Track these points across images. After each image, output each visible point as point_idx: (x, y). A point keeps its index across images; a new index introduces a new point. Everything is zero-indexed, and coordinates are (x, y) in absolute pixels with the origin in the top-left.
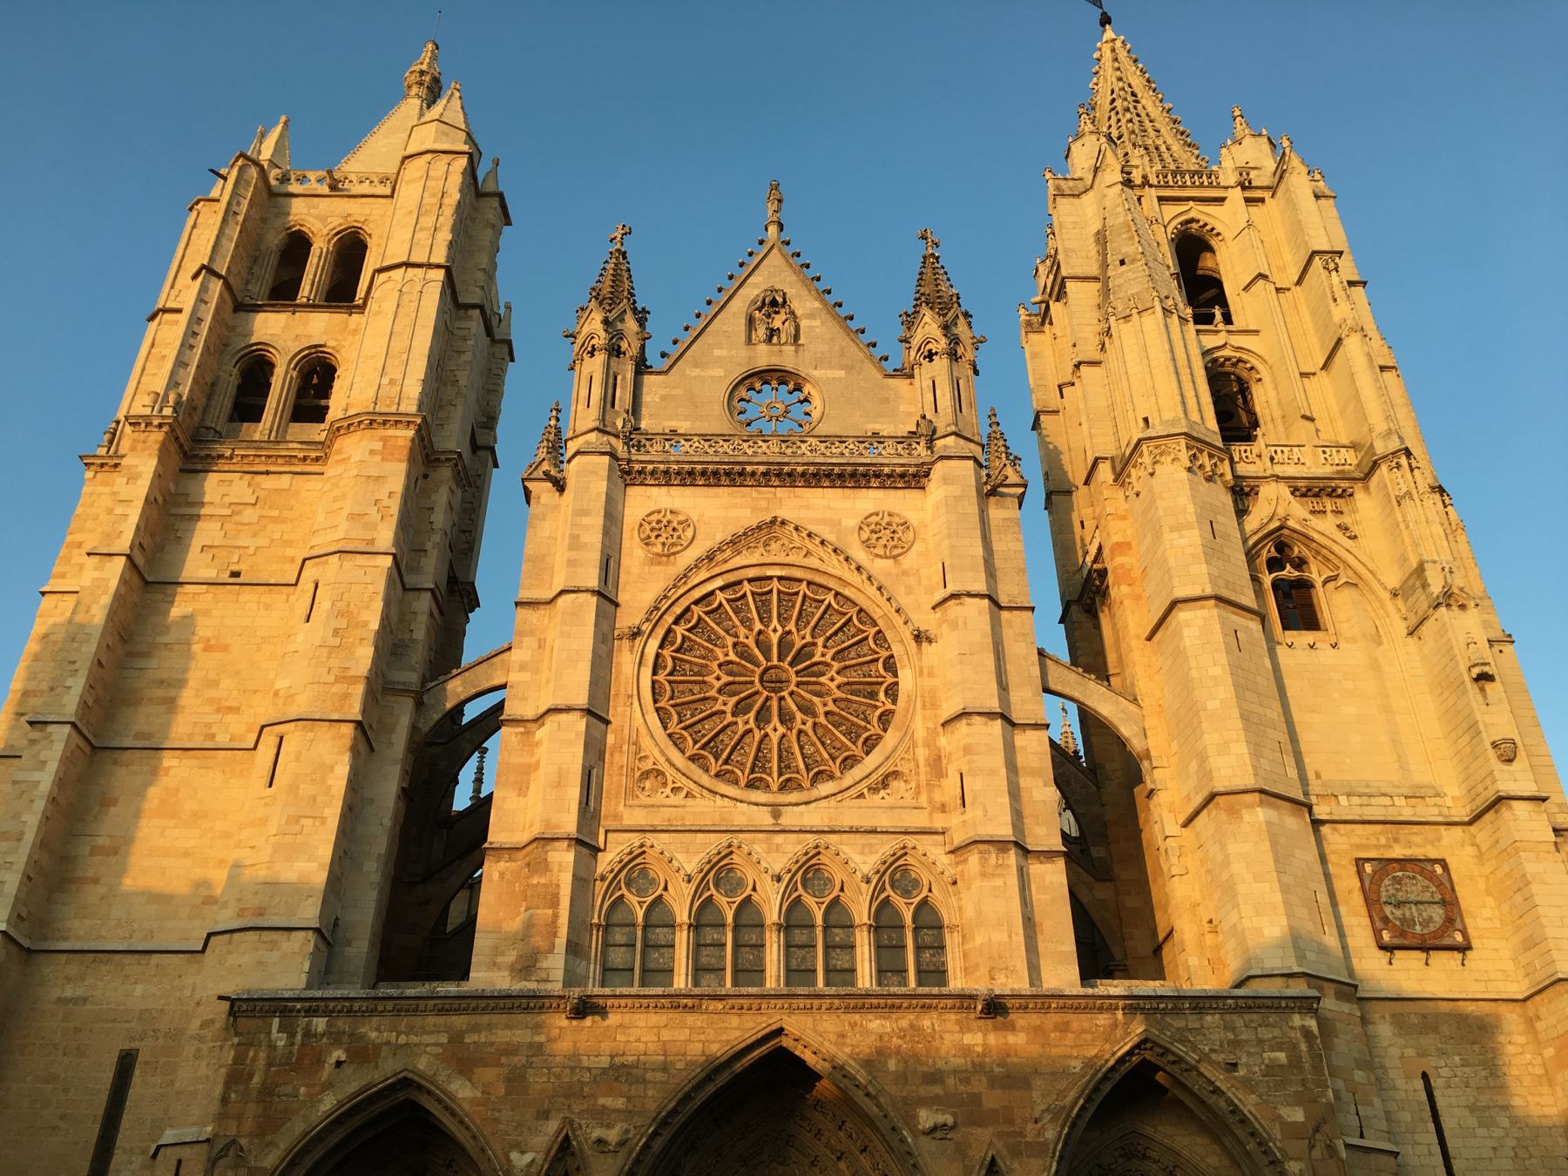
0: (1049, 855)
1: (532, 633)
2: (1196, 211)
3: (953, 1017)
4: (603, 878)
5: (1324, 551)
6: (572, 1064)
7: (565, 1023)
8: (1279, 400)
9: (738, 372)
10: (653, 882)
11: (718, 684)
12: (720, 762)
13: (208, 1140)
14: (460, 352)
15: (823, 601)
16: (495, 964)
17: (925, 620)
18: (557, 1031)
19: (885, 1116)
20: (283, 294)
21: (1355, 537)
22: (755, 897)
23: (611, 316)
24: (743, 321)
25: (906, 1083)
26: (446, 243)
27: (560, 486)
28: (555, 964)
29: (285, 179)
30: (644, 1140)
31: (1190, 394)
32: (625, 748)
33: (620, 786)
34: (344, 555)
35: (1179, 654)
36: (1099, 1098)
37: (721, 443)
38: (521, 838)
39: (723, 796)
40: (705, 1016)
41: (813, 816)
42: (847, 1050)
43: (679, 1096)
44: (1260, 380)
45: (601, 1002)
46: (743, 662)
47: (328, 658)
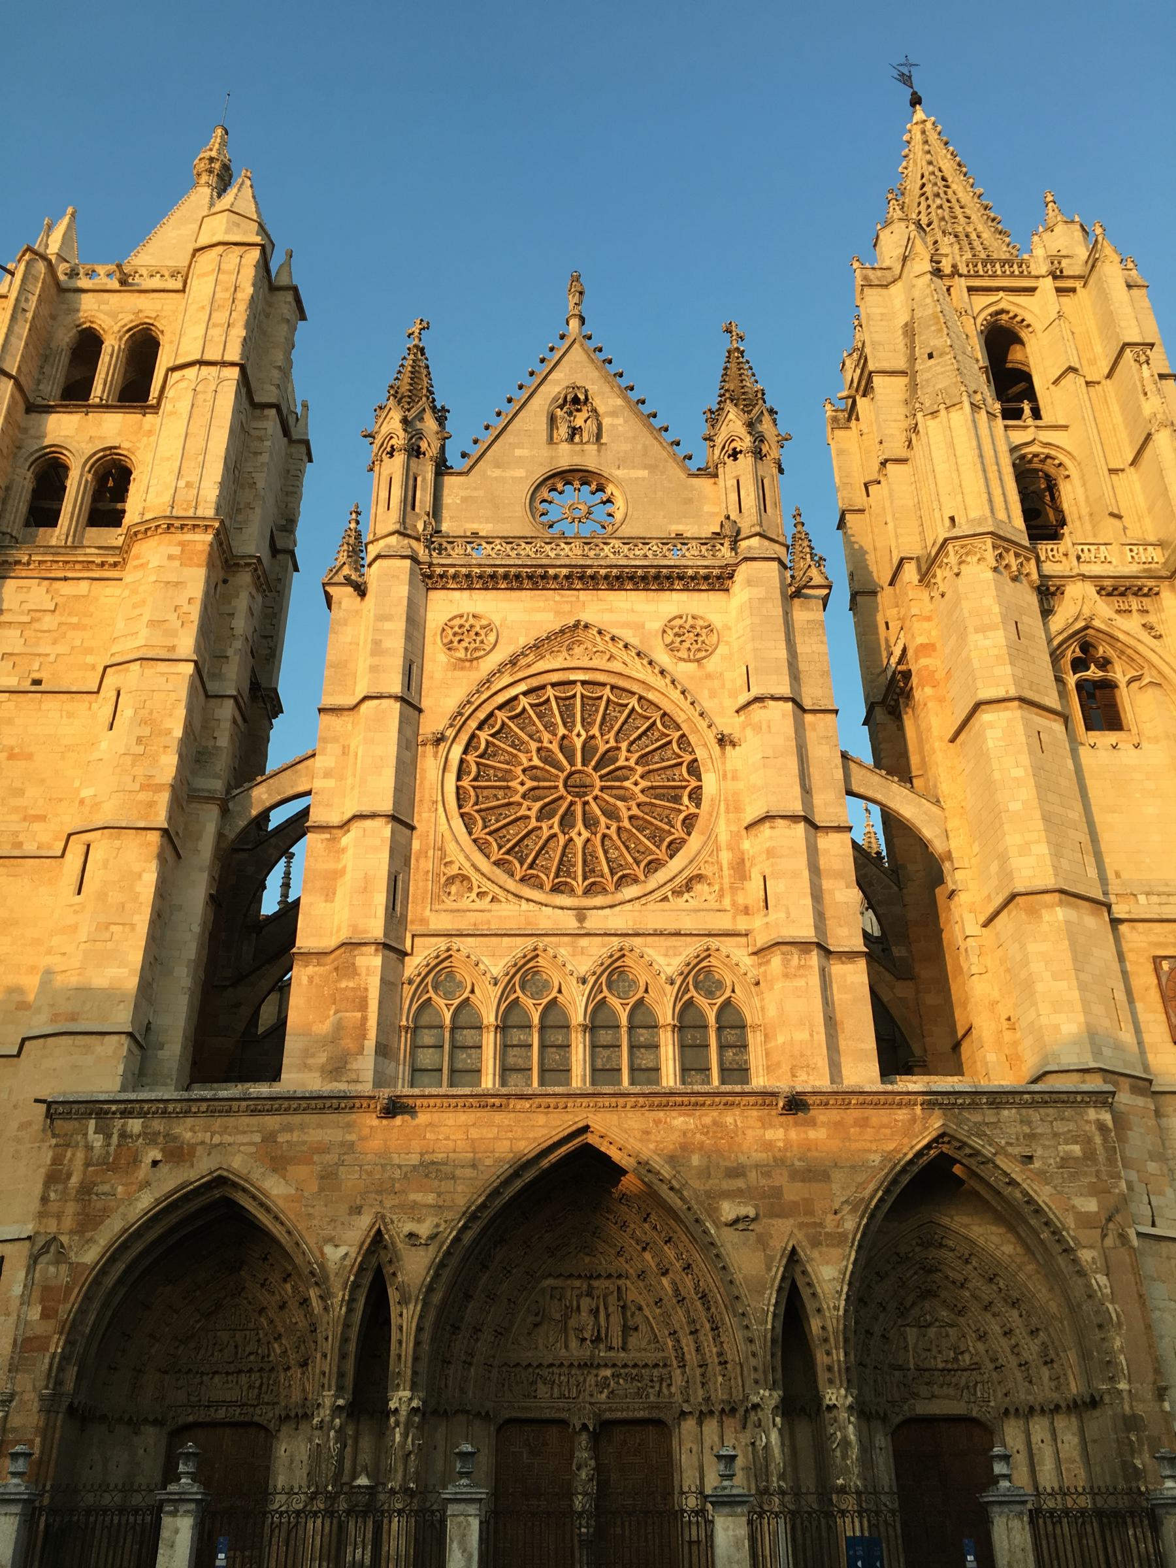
0: (851, 956)
1: (335, 739)
2: (1006, 301)
3: (755, 1113)
4: (410, 982)
5: (1129, 651)
6: (383, 1162)
7: (376, 1122)
8: (1087, 497)
9: (539, 473)
10: (460, 985)
11: (522, 789)
12: (525, 866)
13: (29, 1238)
14: (256, 454)
15: (626, 705)
16: (305, 1066)
17: (729, 723)
18: (368, 1130)
19: (689, 1209)
21: (1161, 636)
22: (561, 999)
23: (411, 415)
24: (544, 420)
25: (709, 1177)
26: (240, 340)
27: (361, 591)
28: (365, 1065)
29: (73, 274)
30: (454, 1233)
31: (997, 492)
32: (431, 853)
33: (426, 892)
34: (144, 662)
35: (982, 756)
36: (898, 1190)
37: (524, 545)
39: (528, 900)
40: (512, 1115)
41: (617, 920)
42: (652, 1146)
43: (488, 1191)
44: (1068, 477)
45: (410, 1102)
46: (547, 767)
47: (133, 766)
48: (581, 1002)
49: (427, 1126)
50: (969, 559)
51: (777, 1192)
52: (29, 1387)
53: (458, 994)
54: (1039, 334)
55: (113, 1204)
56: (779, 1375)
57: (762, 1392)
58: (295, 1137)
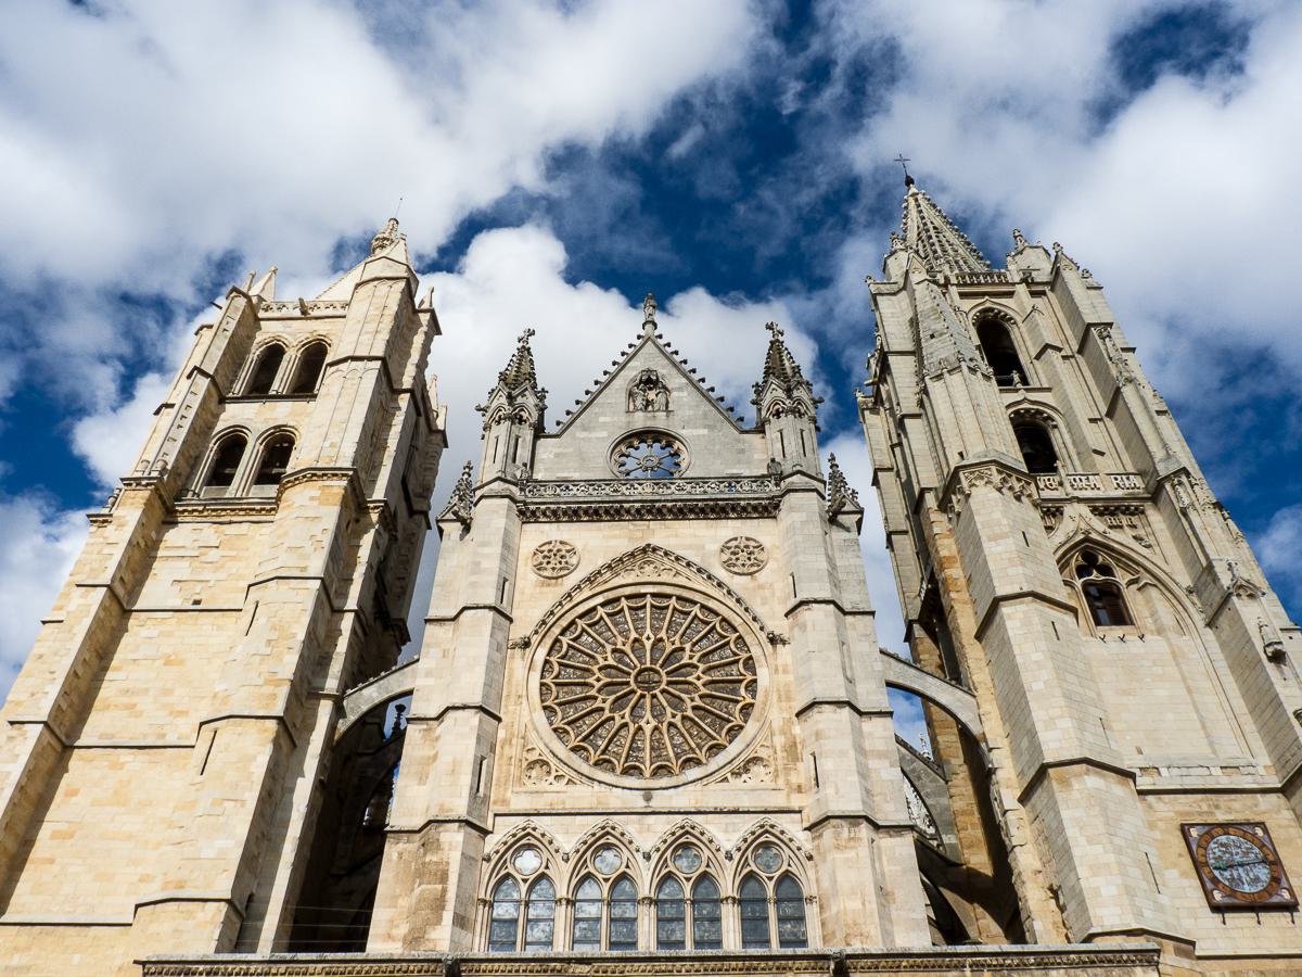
9: (619, 433)
11: (598, 685)
12: (598, 753)
17: (779, 625)
20: (259, 390)
24: (623, 396)
32: (514, 741)
35: (1005, 643)
37: (603, 487)
38: (418, 823)
39: (600, 782)
47: (260, 664)
48: (647, 876)
50: (977, 483)
54: (1020, 324)
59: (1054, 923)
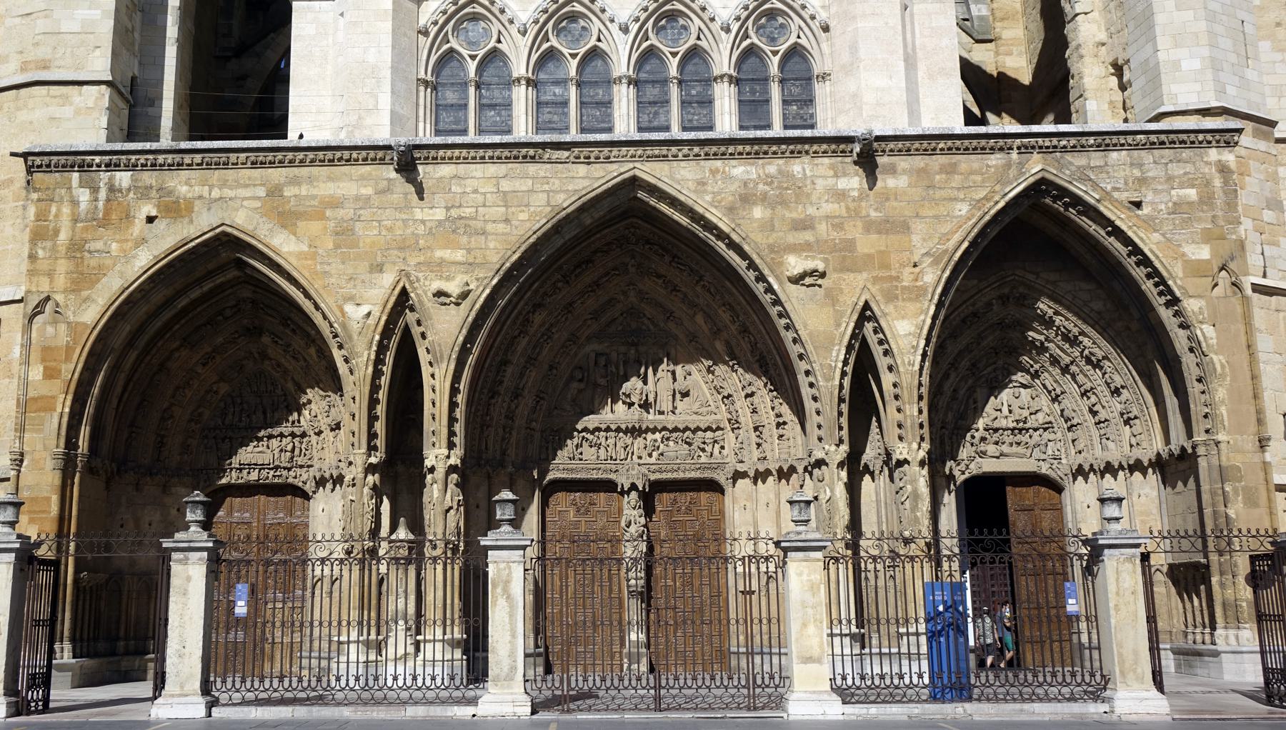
3: (826, 160)
6: (404, 216)
7: (393, 175)
18: (385, 183)
30: (488, 291)
40: (548, 166)
43: (523, 248)
49: (451, 178)
51: (850, 245)
52: (39, 447)
53: (483, 44)
55: (108, 262)
56: (845, 433)
57: (827, 447)
58: (304, 190)
59: (1111, 102)
